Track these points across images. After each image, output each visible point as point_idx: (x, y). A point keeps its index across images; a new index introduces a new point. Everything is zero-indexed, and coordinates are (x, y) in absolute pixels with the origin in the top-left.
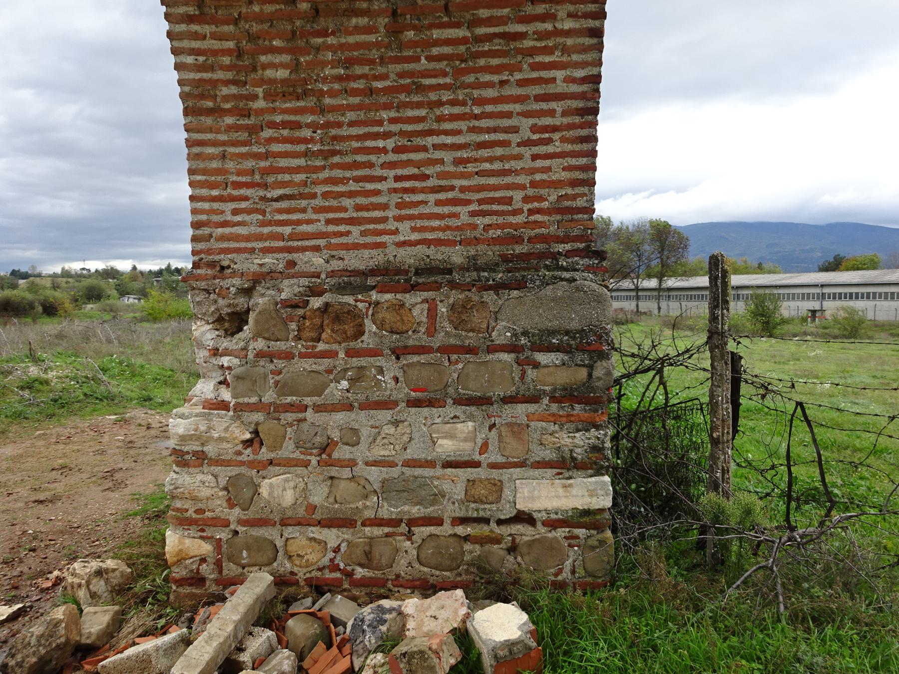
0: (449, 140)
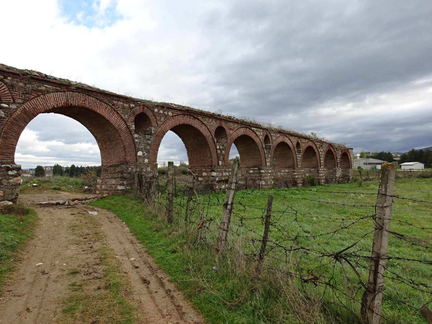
0: (116, 152)
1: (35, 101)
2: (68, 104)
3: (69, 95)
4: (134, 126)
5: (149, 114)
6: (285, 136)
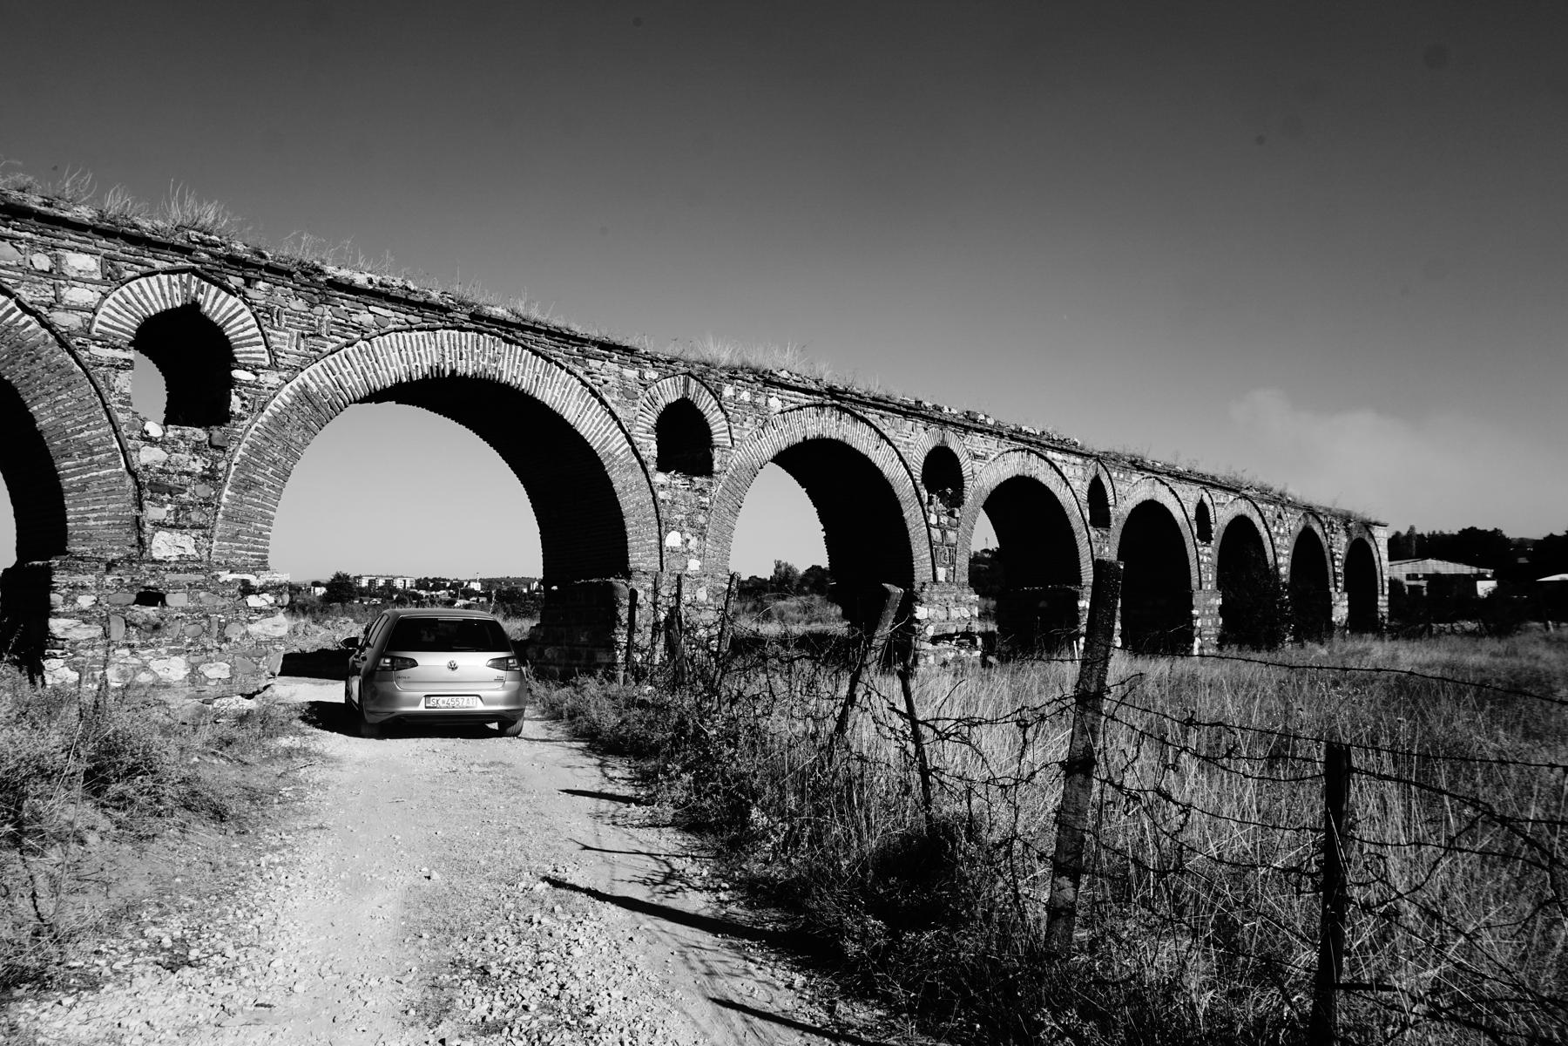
1: (338, 360)
2: (443, 371)
3: (446, 342)
4: (654, 446)
5: (705, 403)
6: (1157, 482)
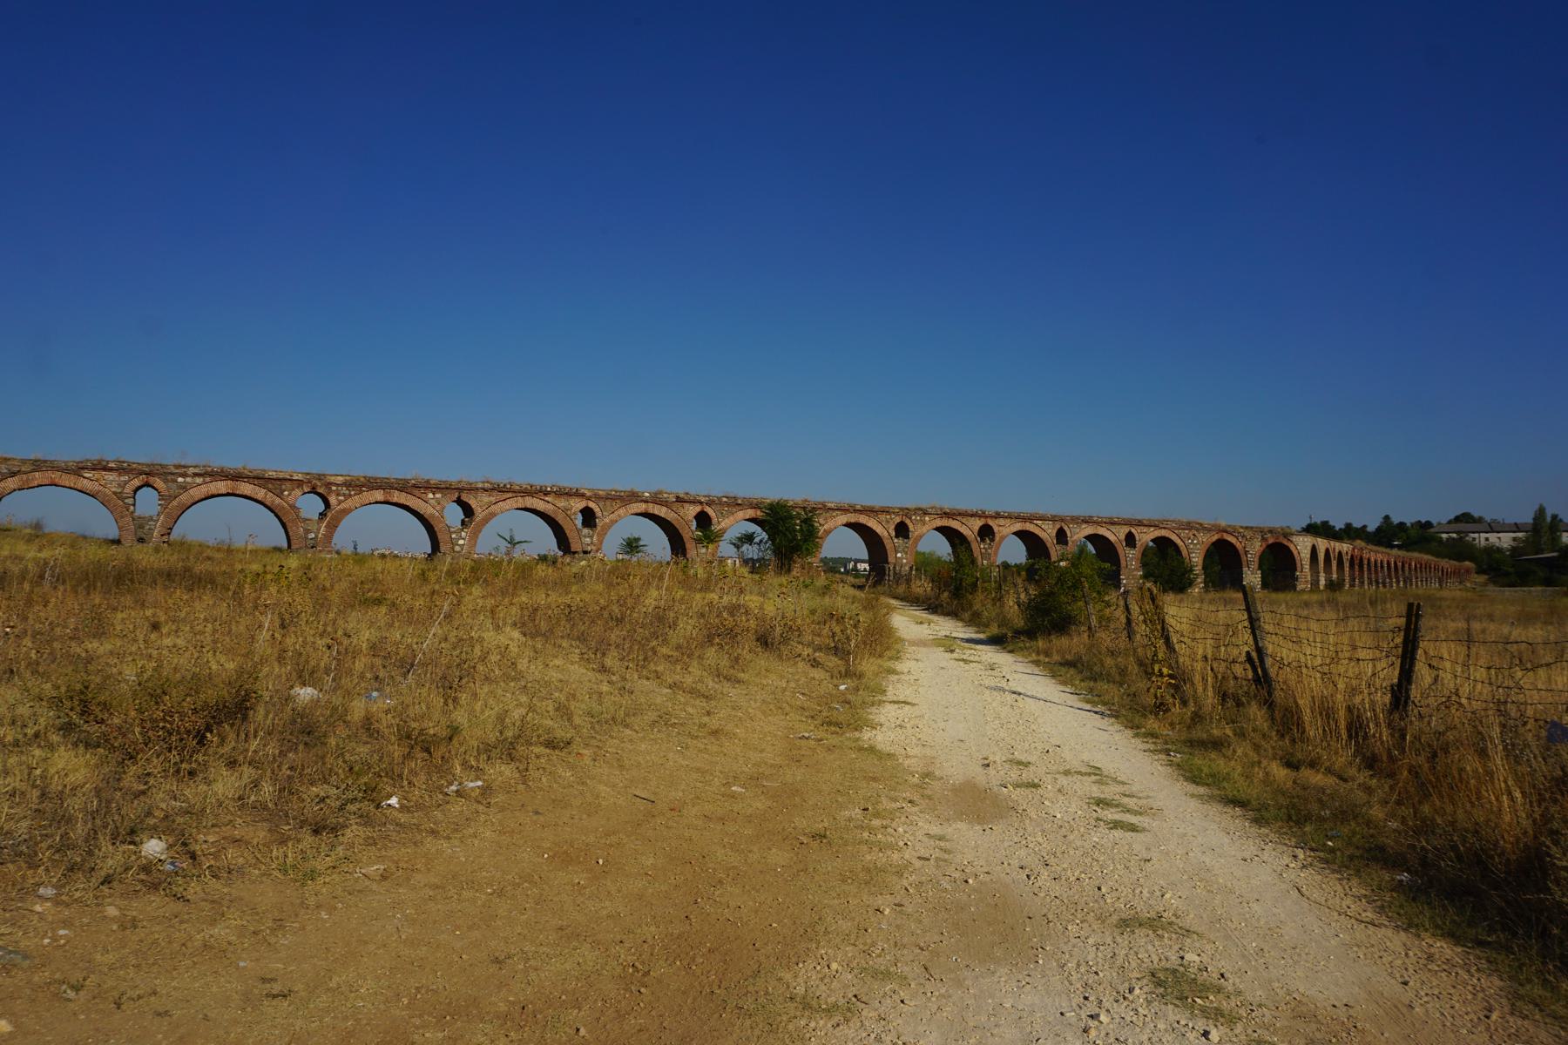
5: (908, 521)
